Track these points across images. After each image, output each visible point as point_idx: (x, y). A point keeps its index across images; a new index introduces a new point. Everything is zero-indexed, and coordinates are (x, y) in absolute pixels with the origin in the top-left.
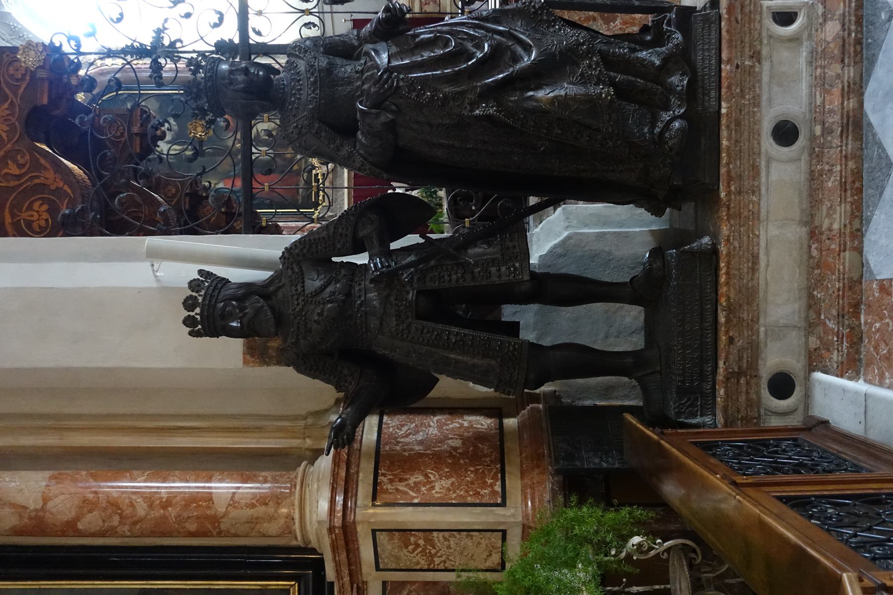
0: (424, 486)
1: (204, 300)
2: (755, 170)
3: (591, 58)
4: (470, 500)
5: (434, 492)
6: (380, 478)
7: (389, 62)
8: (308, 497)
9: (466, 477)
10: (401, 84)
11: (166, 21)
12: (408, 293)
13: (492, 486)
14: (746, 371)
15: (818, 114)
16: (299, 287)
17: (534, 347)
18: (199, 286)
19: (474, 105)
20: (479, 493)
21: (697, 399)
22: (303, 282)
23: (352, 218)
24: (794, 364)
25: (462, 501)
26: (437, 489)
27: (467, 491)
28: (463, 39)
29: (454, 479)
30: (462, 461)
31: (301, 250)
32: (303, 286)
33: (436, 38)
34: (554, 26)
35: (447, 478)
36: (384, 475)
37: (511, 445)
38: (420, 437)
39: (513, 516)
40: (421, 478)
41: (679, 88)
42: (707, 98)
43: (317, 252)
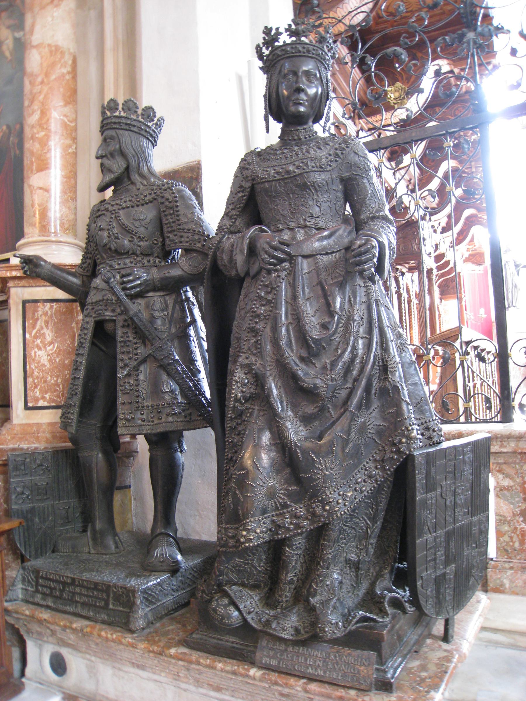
0: (41, 342)
1: (116, 117)
3: (307, 518)
4: (30, 380)
5: (36, 350)
6: (48, 305)
7: (305, 257)
8: (37, 247)
9: (51, 376)
10: (274, 275)
11: (509, 31)
12: (113, 311)
13: (43, 398)
16: (128, 204)
18: (129, 109)
19: (249, 369)
20: (36, 387)
21: (32, 587)
22: (133, 207)
23: (199, 245)
25: (28, 374)
26: (39, 353)
27: (37, 377)
28: (337, 349)
29: (48, 366)
30: (66, 372)
31: (167, 199)
32: (128, 208)
33: (331, 314)
34: (376, 468)
35: (50, 361)
36: (51, 307)
39: (18, 416)
40: (49, 338)
41: (274, 626)
42: (271, 653)
43: (166, 215)
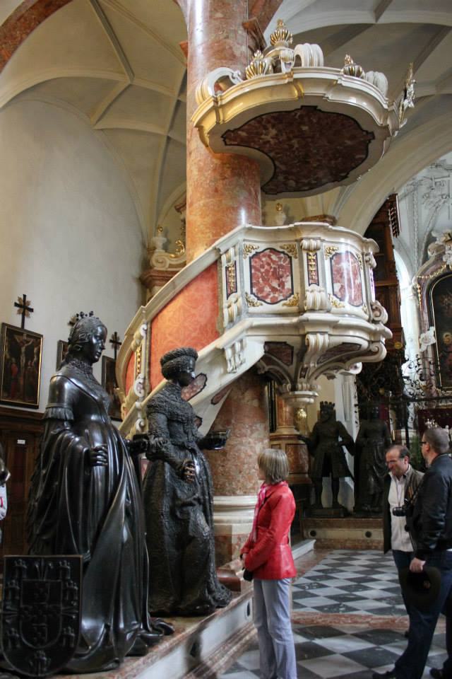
2: (359, 527)
14: (317, 525)
15: (372, 542)
17: (321, 480)
24: (317, 537)
37: (301, 475)
38: (302, 454)
